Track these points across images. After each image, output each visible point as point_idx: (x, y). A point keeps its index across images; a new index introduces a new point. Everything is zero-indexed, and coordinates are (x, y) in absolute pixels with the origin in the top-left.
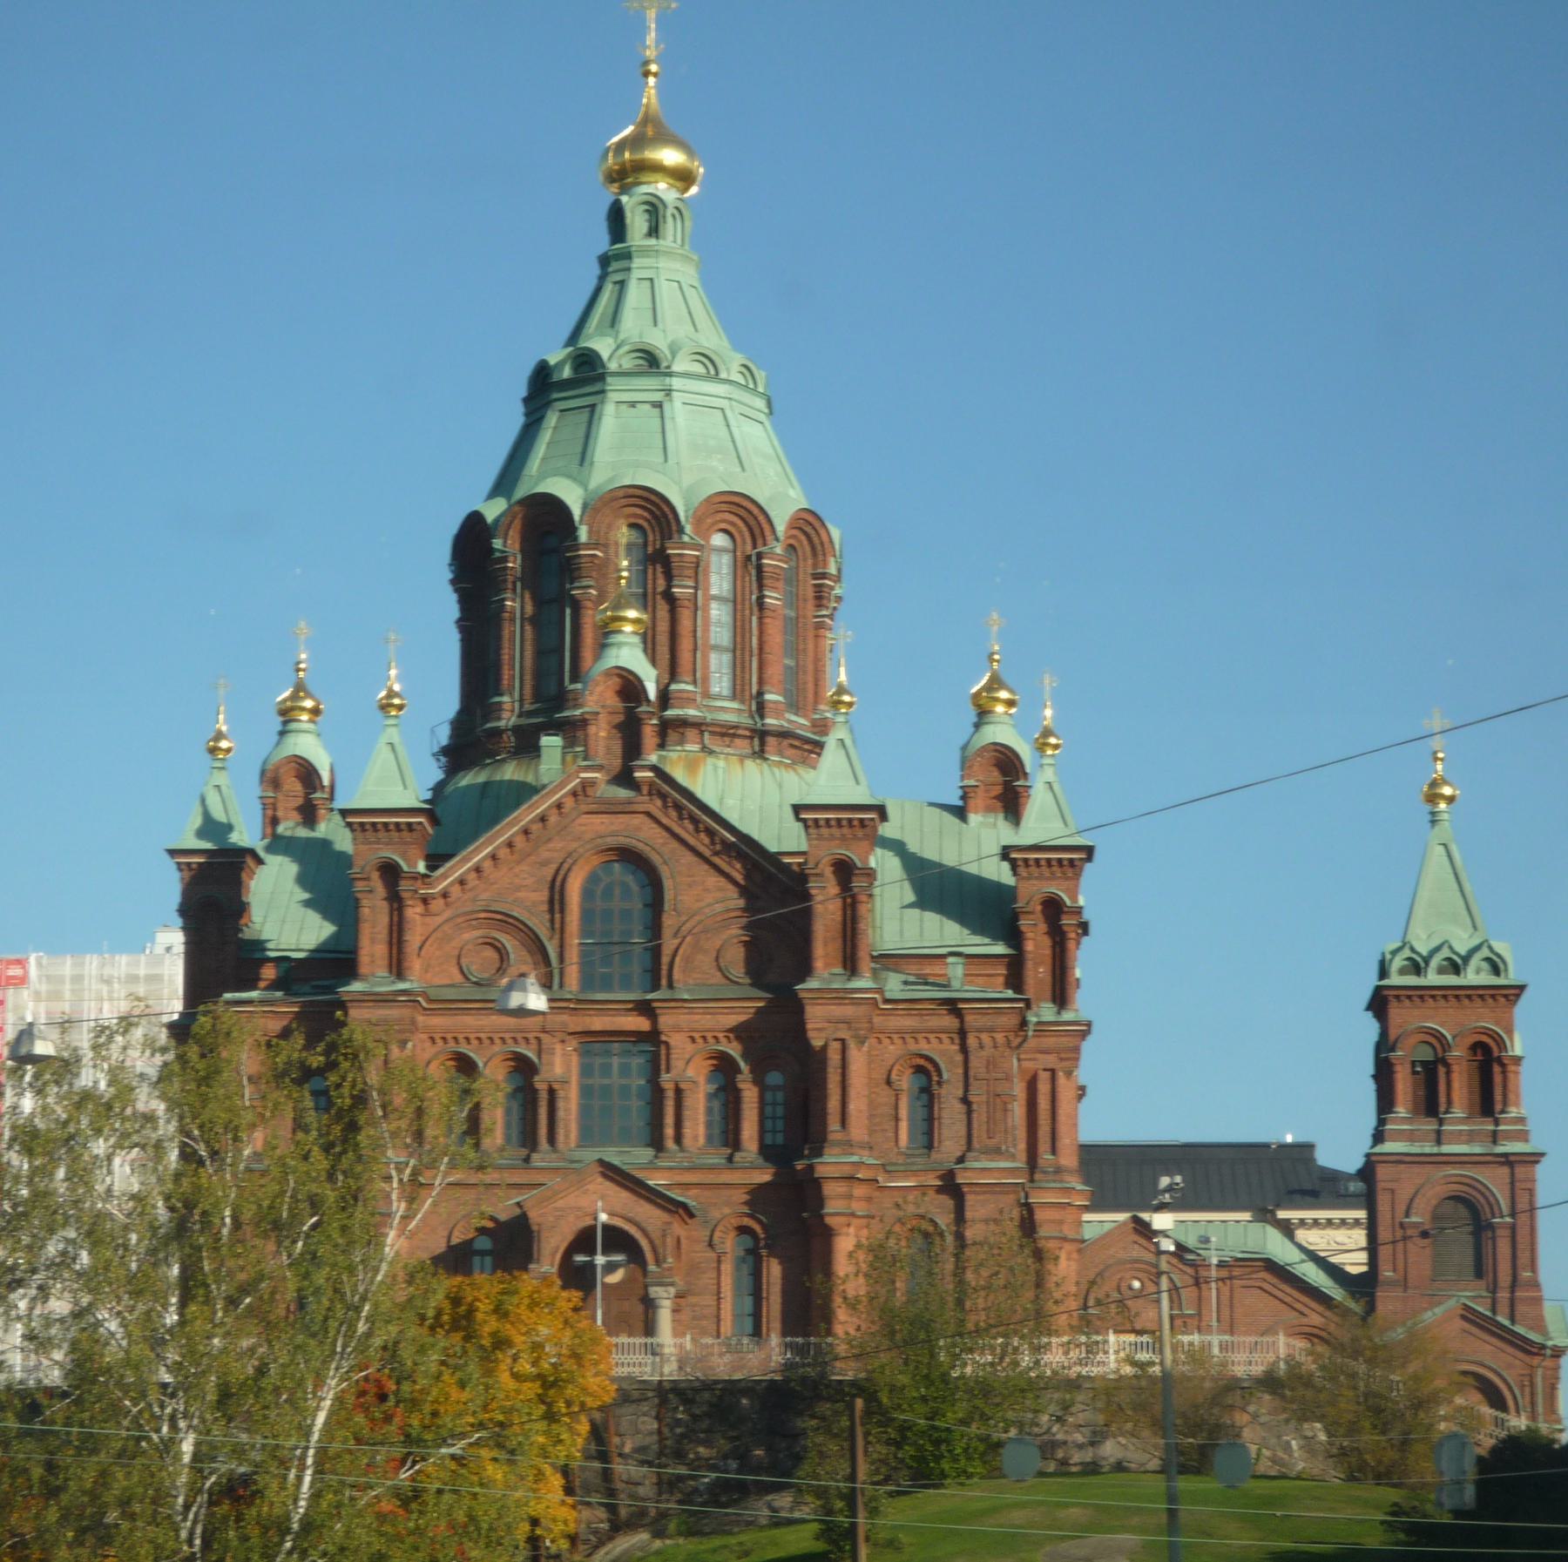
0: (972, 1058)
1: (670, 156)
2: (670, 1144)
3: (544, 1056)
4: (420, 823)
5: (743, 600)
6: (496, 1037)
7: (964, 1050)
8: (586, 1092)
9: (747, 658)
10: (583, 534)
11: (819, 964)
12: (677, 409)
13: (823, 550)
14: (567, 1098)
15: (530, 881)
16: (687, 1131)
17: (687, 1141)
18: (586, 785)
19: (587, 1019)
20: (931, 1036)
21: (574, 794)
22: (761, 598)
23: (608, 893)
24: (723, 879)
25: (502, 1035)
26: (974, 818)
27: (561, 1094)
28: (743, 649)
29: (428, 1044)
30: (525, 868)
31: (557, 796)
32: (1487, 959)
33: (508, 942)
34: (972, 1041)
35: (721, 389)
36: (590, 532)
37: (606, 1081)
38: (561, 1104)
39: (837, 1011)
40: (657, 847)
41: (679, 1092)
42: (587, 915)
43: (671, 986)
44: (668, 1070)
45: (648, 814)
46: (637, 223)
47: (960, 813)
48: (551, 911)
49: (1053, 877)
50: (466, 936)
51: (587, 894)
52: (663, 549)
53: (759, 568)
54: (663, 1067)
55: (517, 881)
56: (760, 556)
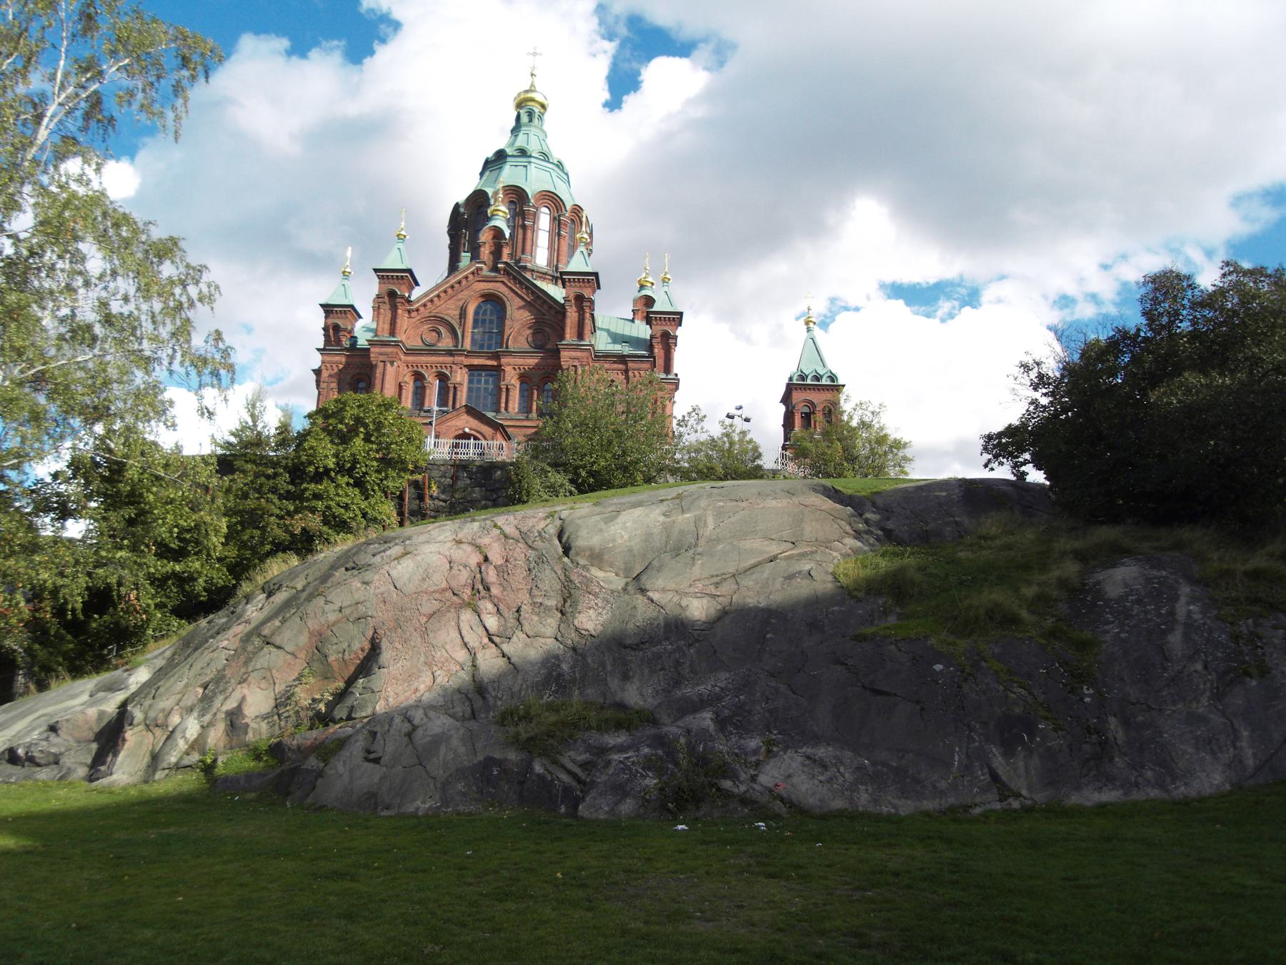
2: (503, 410)
3: (453, 374)
6: (434, 365)
8: (470, 390)
10: (492, 202)
11: (568, 336)
16: (510, 405)
18: (479, 269)
21: (473, 273)
22: (559, 230)
26: (636, 321)
27: (459, 389)
29: (406, 368)
32: (829, 376)
34: (630, 374)
35: (551, 166)
38: (459, 393)
39: (573, 354)
41: (508, 389)
42: (476, 322)
43: (507, 347)
45: (502, 282)
46: (525, 119)
47: (633, 321)
48: (460, 318)
49: (666, 325)
51: (476, 313)
53: (559, 220)
56: (559, 216)
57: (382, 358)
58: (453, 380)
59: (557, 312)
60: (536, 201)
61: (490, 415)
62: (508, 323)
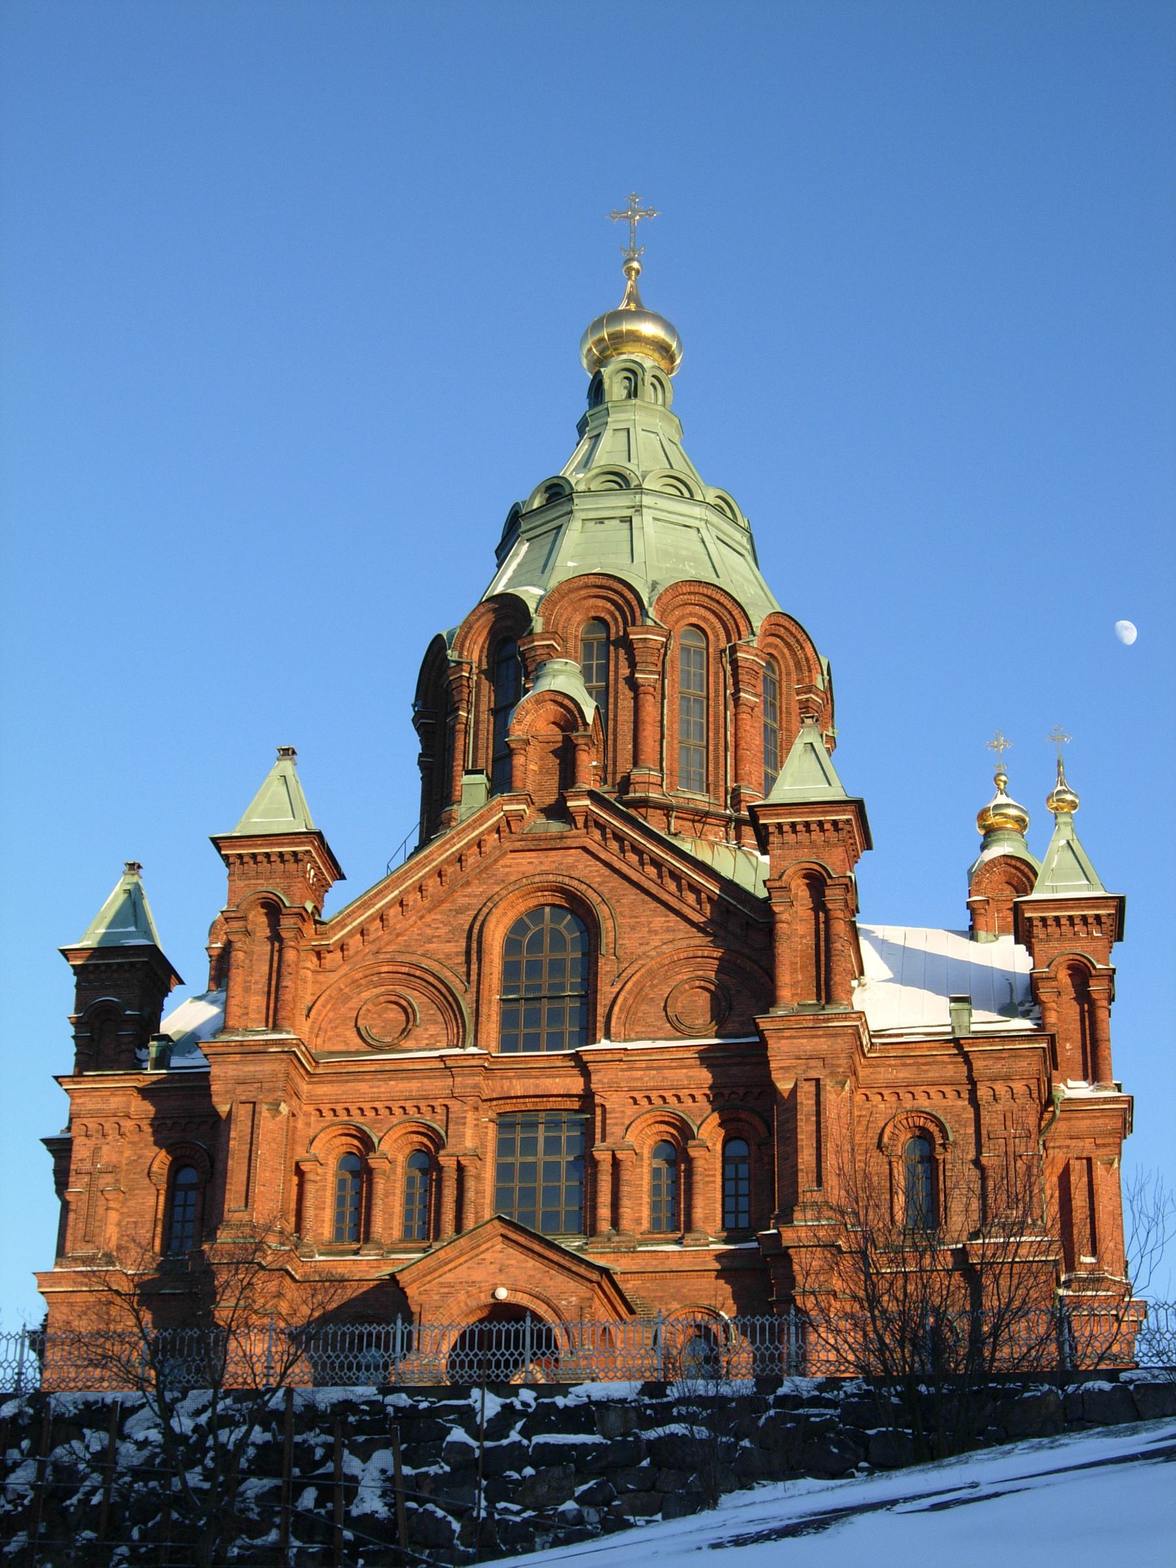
0: (983, 1113)
1: (649, 329)
2: (605, 1226)
4: (308, 852)
5: (717, 696)
7: (974, 1101)
8: (503, 1172)
9: (722, 753)
10: (538, 625)
11: (785, 993)
12: (646, 523)
13: (809, 667)
14: (478, 1178)
15: (443, 931)
16: (626, 1211)
17: (626, 1223)
18: (508, 819)
19: (506, 1083)
20: (932, 1091)
22: (737, 690)
23: (536, 943)
24: (673, 917)
25: (402, 1103)
26: (982, 934)
27: (471, 1171)
28: (717, 745)
30: (439, 917)
31: (477, 832)
33: (416, 999)
34: (983, 1092)
35: (697, 511)
36: (546, 623)
37: (530, 1159)
39: (807, 1045)
40: (595, 886)
41: (616, 1164)
42: (510, 970)
44: (603, 1139)
45: (585, 849)
46: (615, 388)
48: (468, 962)
50: (366, 995)
51: (511, 945)
52: (626, 634)
53: (734, 663)
54: (598, 1136)
55: (429, 931)
57: (243, 1093)
58: (452, 1146)
59: (748, 925)
60: (663, 614)
61: (572, 1244)
62: (605, 966)
